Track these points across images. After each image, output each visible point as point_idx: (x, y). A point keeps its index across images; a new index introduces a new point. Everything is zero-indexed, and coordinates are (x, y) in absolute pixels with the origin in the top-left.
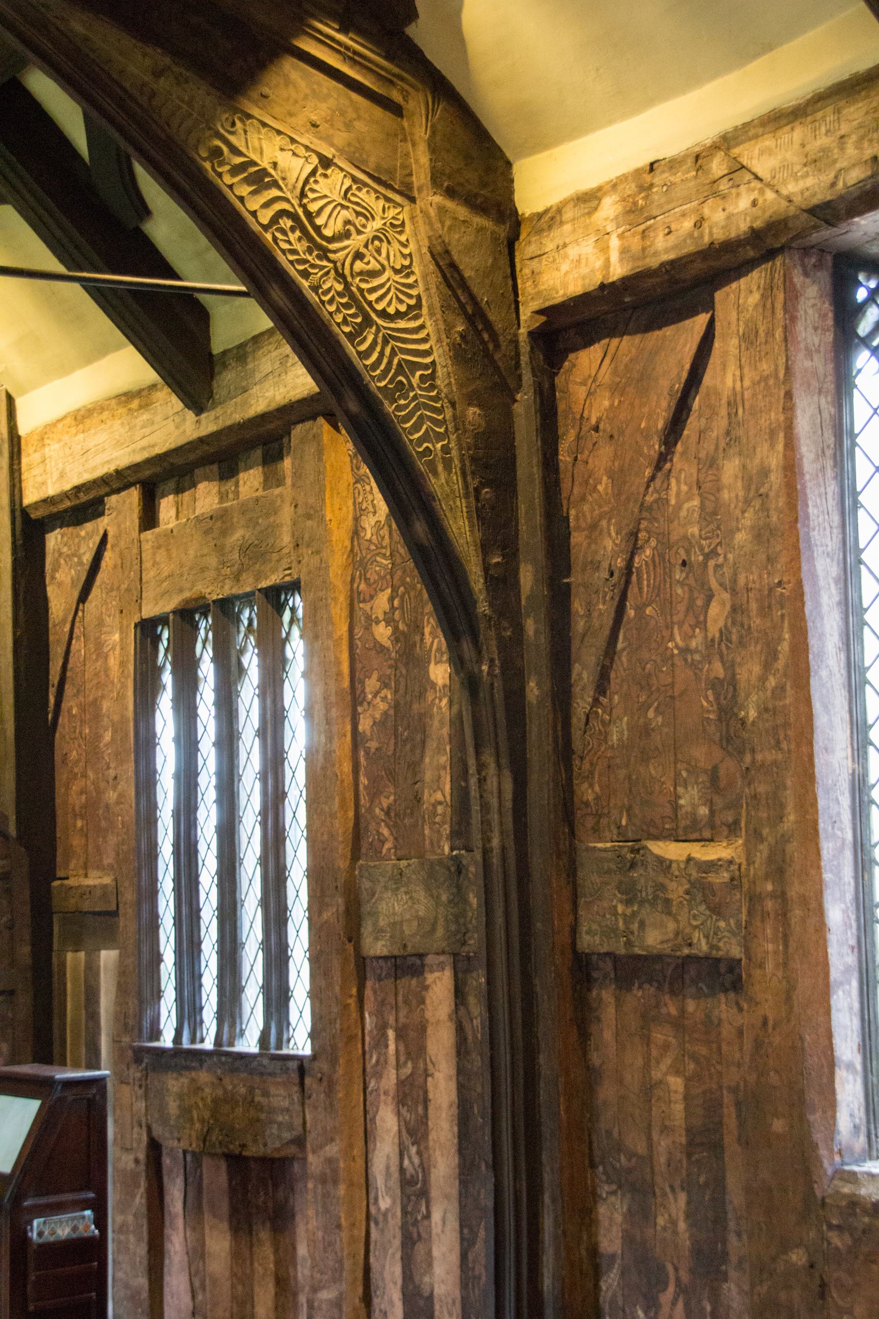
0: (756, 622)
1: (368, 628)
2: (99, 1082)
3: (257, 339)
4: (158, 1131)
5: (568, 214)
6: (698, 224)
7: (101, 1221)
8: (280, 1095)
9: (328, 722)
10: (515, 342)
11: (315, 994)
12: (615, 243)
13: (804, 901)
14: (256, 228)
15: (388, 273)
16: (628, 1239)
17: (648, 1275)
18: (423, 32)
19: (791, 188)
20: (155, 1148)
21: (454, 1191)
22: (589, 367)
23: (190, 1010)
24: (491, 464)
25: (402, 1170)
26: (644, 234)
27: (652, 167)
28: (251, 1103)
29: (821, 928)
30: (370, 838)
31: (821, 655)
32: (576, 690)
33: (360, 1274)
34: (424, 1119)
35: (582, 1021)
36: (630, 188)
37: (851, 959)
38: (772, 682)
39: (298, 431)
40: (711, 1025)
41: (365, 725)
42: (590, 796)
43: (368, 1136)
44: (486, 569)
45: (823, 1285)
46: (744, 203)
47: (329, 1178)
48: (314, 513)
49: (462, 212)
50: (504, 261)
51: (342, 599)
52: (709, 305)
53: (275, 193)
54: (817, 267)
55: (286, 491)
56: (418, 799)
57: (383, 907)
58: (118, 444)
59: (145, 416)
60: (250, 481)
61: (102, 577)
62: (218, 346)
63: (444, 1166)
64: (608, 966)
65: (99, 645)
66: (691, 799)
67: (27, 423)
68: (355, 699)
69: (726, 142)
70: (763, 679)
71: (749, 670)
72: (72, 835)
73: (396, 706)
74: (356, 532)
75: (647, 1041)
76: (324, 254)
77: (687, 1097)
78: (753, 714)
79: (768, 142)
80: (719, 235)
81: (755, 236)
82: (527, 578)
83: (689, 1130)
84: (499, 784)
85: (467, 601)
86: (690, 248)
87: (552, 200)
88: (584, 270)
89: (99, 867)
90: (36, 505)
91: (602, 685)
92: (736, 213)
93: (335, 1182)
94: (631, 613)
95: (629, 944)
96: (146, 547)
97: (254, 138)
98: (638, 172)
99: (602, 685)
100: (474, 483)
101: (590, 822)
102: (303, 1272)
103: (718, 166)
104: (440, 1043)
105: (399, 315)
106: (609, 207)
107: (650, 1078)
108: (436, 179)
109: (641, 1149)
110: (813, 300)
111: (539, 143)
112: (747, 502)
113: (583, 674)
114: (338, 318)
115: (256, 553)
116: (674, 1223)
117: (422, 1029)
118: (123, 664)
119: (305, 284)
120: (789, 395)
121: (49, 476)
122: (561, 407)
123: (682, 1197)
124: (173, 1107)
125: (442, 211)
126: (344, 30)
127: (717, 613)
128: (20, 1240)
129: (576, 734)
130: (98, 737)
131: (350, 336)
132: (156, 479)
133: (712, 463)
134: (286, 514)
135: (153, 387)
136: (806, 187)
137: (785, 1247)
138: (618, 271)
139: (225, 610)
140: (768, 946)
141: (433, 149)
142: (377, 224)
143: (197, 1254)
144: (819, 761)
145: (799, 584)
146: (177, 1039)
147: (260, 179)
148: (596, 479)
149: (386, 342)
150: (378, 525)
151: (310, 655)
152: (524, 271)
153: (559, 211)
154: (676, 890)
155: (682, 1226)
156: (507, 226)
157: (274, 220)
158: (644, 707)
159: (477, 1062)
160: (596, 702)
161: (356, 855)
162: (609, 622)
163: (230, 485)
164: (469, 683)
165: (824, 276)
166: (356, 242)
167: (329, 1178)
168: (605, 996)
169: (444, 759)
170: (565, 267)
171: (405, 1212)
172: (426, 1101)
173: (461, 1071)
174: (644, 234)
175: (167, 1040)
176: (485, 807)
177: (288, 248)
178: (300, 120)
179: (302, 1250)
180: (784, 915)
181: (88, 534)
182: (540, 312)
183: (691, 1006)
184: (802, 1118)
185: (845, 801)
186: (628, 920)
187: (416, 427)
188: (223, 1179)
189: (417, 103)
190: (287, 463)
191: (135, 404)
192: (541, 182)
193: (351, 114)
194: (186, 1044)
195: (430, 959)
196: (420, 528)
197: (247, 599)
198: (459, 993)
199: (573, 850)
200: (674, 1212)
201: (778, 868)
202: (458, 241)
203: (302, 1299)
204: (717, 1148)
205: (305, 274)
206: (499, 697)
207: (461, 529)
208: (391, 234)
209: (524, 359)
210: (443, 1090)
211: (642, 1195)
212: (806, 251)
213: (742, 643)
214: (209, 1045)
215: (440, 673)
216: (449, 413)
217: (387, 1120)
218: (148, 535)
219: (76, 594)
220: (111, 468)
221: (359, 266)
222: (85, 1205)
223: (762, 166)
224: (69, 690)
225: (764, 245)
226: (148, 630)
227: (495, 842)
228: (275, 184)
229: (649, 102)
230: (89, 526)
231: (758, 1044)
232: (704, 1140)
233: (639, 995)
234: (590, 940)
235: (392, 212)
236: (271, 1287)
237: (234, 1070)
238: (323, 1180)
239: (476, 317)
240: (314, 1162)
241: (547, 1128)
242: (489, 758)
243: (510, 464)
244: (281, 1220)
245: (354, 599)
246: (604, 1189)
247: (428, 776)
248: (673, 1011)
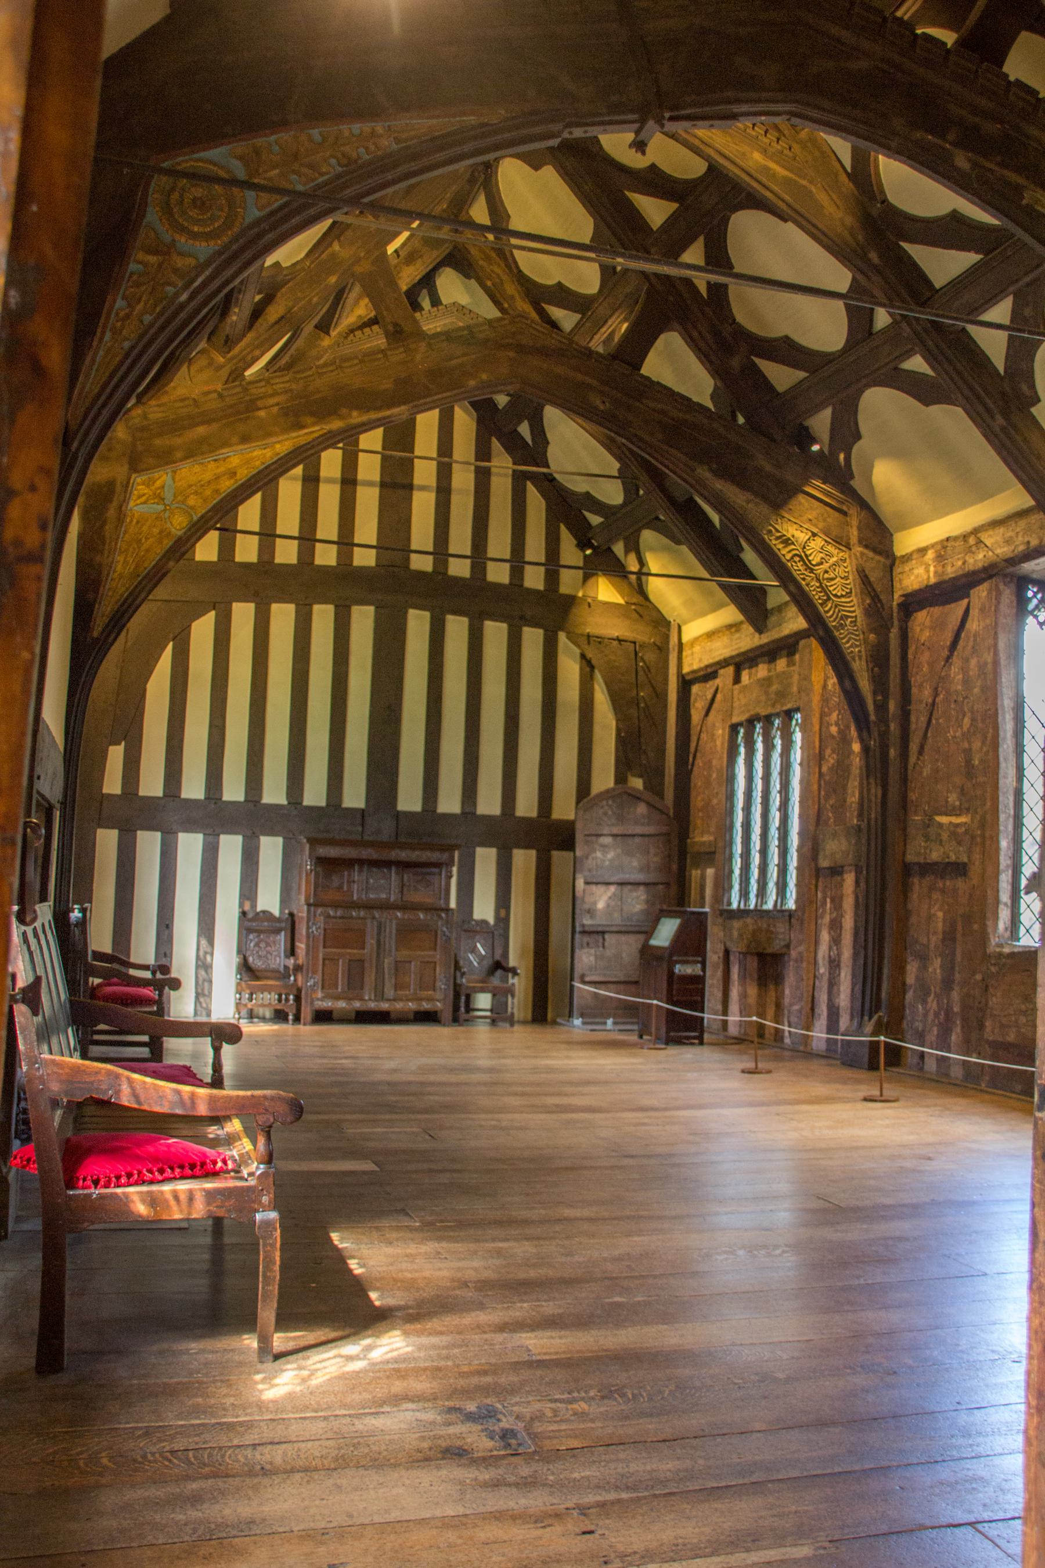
0: (980, 725)
1: (828, 728)
2: (706, 913)
3: (786, 604)
4: (728, 944)
5: (915, 556)
6: (964, 563)
7: (704, 969)
8: (781, 928)
9: (809, 767)
10: (891, 608)
11: (798, 885)
12: (932, 569)
13: (991, 837)
14: (784, 560)
15: (838, 579)
16: (917, 978)
17: (924, 990)
18: (856, 483)
19: (998, 551)
20: (727, 953)
21: (850, 964)
22: (922, 618)
23: (744, 894)
24: (879, 658)
25: (830, 957)
26: (943, 566)
27: (948, 539)
28: (768, 931)
29: (997, 849)
30: (824, 818)
31: (1005, 738)
32: (911, 753)
33: (810, 999)
34: (840, 935)
35: (905, 890)
36: (939, 547)
37: (1009, 862)
38: (985, 749)
39: (802, 643)
40: (955, 890)
41: (824, 769)
42: (914, 798)
43: (817, 943)
44: (875, 701)
45: (987, 986)
46: (981, 556)
47: (800, 959)
48: (807, 678)
49: (871, 554)
50: (888, 575)
51: (817, 715)
52: (968, 596)
53: (793, 547)
54: (1011, 581)
55: (796, 668)
56: (845, 801)
57: (828, 847)
58: (725, 647)
59: (737, 635)
60: (781, 664)
61: (715, 706)
62: (769, 606)
63: (847, 954)
64: (916, 868)
65: (713, 735)
66: (953, 798)
67: (685, 638)
68: (821, 757)
69: (976, 531)
70: (981, 749)
71: (977, 745)
72: (697, 818)
73: (838, 761)
74: (825, 686)
75: (930, 898)
76: (812, 571)
77: (944, 921)
78: (977, 762)
79: (991, 532)
80: (971, 568)
81: (985, 569)
82: (892, 706)
83: (944, 933)
84: (876, 791)
85: (866, 715)
86: (961, 573)
87: (909, 550)
88: (920, 579)
89: (709, 833)
90: (688, 674)
91: (921, 751)
92: (978, 559)
93: (802, 962)
94: (934, 721)
95: (925, 858)
96: (736, 692)
97: (785, 526)
98: (942, 541)
99: (921, 751)
100: (871, 666)
101: (913, 809)
102: (787, 1001)
103: (972, 541)
104: (848, 904)
105: (842, 596)
106: (930, 555)
107: (930, 912)
108: (860, 541)
109: (925, 941)
110: (1008, 595)
111: (905, 527)
112: (979, 676)
113: (914, 747)
114: (817, 597)
115: (782, 695)
116: (935, 970)
117: (841, 897)
118: (723, 743)
119: (804, 583)
120: (996, 633)
121: (694, 661)
122: (910, 635)
123: (939, 960)
124: (735, 934)
125: (862, 554)
126: (824, 483)
127: (967, 721)
128: (671, 974)
129: (910, 772)
130: (710, 776)
131: (821, 604)
132: (741, 662)
133: (967, 660)
134: (796, 677)
135: (741, 623)
136: (1003, 551)
137: (974, 973)
138: (933, 580)
139: (768, 720)
140: (977, 857)
141: (859, 529)
142: (835, 559)
143: (744, 996)
144: (1001, 782)
145: (997, 710)
146: (739, 905)
147: (787, 542)
148: (922, 664)
149: (836, 606)
150: (834, 684)
151: (803, 740)
152: (896, 579)
153: (911, 554)
154: (945, 836)
155: (938, 971)
156: (891, 561)
157: (792, 558)
158: (937, 760)
159: (862, 907)
160: (918, 759)
161: (818, 824)
162: (924, 725)
163: (772, 666)
164: (866, 749)
165: (1013, 586)
166: (825, 566)
167: (800, 959)
168: (916, 880)
169: (856, 783)
170: (912, 578)
171: (830, 974)
172: (841, 927)
173: (856, 914)
174: (943, 566)
175: (735, 906)
176: (870, 801)
177: (797, 569)
178: (805, 518)
179: (787, 992)
180: (983, 843)
181: (711, 686)
182: (903, 596)
183: (948, 883)
184: (985, 925)
185: (1011, 798)
186: (925, 848)
187: (848, 642)
188: (755, 964)
189: (853, 510)
190: (797, 657)
191: (733, 630)
192: (907, 542)
193: (826, 515)
194: (742, 906)
195: (845, 868)
196: (847, 683)
197: (777, 715)
198: (857, 883)
199: (905, 821)
200: (936, 966)
201: (982, 825)
202: (868, 566)
203: (786, 1012)
204: (954, 940)
205: (804, 579)
206: (878, 754)
207: (865, 685)
208: (840, 563)
209: (895, 615)
210: (848, 922)
211: (924, 959)
212: (1005, 576)
213: (974, 734)
214: (752, 907)
215: (856, 747)
216: (862, 636)
217: (825, 936)
218: (736, 686)
219: (703, 713)
220: (722, 657)
221: (826, 576)
222: (698, 962)
223: (988, 542)
224: (698, 755)
225: (989, 573)
226: (734, 729)
227: (873, 816)
228: (793, 543)
229: (947, 514)
230: (711, 683)
231: (971, 895)
232: (949, 937)
233: (929, 879)
234: (910, 858)
235: (841, 554)
236: (774, 1008)
237: (762, 917)
238: (796, 961)
239: (875, 597)
240: (794, 954)
241: (888, 932)
242: (872, 781)
243: (887, 659)
244: (778, 980)
245: (822, 715)
246: (909, 959)
247: (849, 791)
248: (941, 885)
